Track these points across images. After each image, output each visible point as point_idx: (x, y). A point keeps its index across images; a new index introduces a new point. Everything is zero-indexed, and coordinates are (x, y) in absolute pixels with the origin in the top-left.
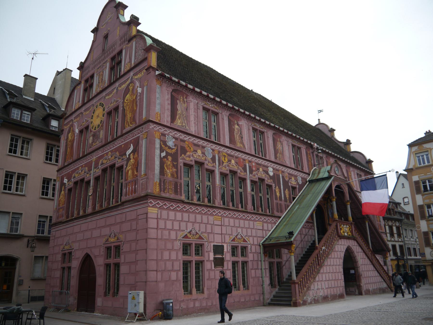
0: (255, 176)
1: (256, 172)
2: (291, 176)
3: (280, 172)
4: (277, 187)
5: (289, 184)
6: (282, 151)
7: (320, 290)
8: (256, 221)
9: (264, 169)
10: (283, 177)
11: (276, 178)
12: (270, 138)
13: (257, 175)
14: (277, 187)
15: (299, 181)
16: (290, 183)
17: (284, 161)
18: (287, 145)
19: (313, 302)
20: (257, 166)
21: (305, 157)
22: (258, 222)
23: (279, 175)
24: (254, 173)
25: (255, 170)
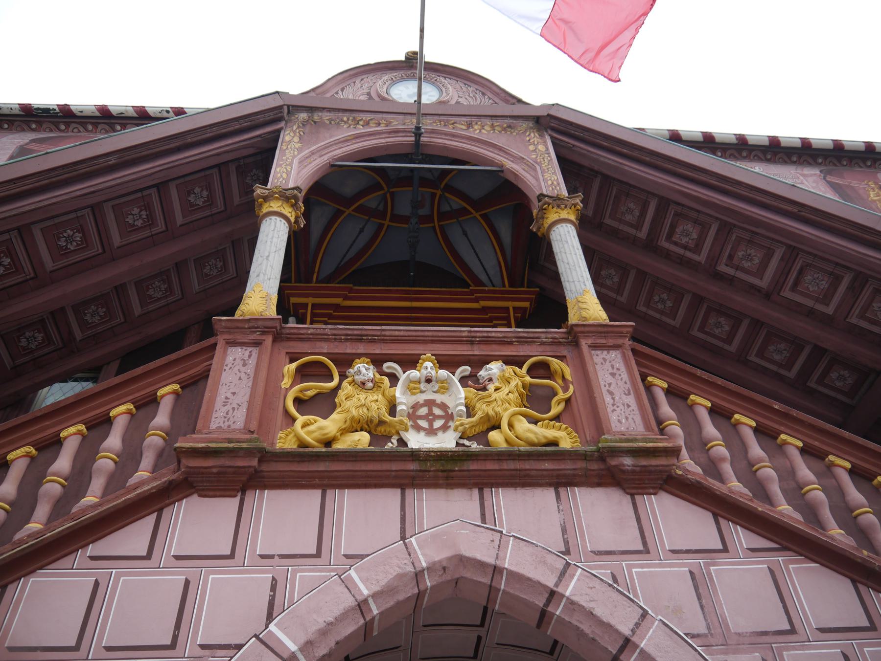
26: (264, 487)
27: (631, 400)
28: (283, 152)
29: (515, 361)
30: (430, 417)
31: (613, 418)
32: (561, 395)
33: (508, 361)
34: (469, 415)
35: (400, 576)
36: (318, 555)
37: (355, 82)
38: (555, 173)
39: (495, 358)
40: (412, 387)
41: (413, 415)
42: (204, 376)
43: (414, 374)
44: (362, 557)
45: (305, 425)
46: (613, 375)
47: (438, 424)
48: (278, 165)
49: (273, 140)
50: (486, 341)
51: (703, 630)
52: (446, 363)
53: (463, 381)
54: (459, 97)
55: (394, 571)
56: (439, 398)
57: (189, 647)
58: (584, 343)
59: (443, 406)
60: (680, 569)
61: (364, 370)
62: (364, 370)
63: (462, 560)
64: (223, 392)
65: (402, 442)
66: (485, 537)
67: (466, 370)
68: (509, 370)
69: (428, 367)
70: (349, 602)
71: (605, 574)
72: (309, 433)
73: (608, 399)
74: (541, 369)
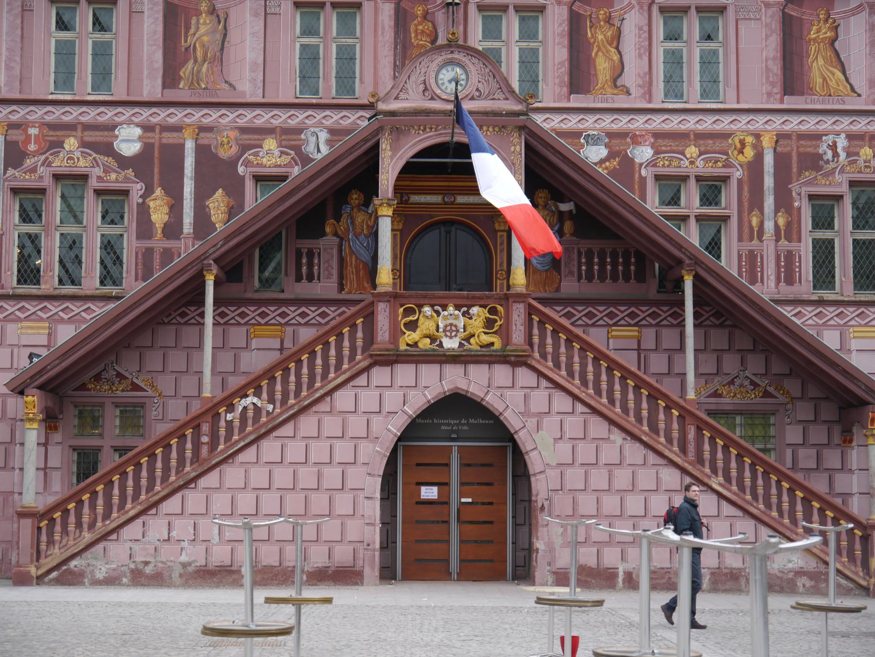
0: (33, 170)
1: (43, 157)
2: (256, 137)
3: (187, 133)
4: (158, 192)
5: (241, 170)
6: (217, 48)
7: (185, 544)
8: (19, 320)
9: (87, 139)
10: (202, 151)
11: (156, 161)
12: (146, 13)
13: (49, 165)
14: (158, 192)
15: (310, 148)
16: (247, 164)
17: (226, 86)
18: (256, 15)
19: (125, 580)
20: (51, 133)
21: (388, 35)
22: (25, 324)
23: (182, 147)
24: (28, 162)
25: (34, 152)
26: (398, 363)
27: (522, 328)
28: (383, 159)
29: (484, 306)
30: (451, 331)
31: (514, 336)
32: (499, 323)
33: (481, 306)
34: (464, 332)
35: (439, 393)
36: (416, 386)
37: (416, 67)
38: (521, 174)
39: (476, 305)
40: (445, 318)
41: (445, 331)
42: (373, 313)
43: (446, 313)
44: (428, 387)
45: (408, 336)
46: (519, 316)
47: (454, 334)
48: (382, 173)
49: (376, 146)
50: (474, 298)
51: (523, 411)
52: (458, 307)
53: (463, 315)
54: (479, 82)
55: (438, 392)
56: (454, 322)
57: (384, 412)
58: (511, 300)
59: (456, 326)
60: (521, 393)
61: (427, 310)
62: (427, 310)
63: (457, 388)
64: (380, 325)
65: (441, 345)
66: (465, 381)
67: (465, 309)
68: (481, 309)
69: (451, 309)
70: (425, 401)
71: (499, 394)
72: (410, 340)
73: (514, 328)
74: (493, 311)
